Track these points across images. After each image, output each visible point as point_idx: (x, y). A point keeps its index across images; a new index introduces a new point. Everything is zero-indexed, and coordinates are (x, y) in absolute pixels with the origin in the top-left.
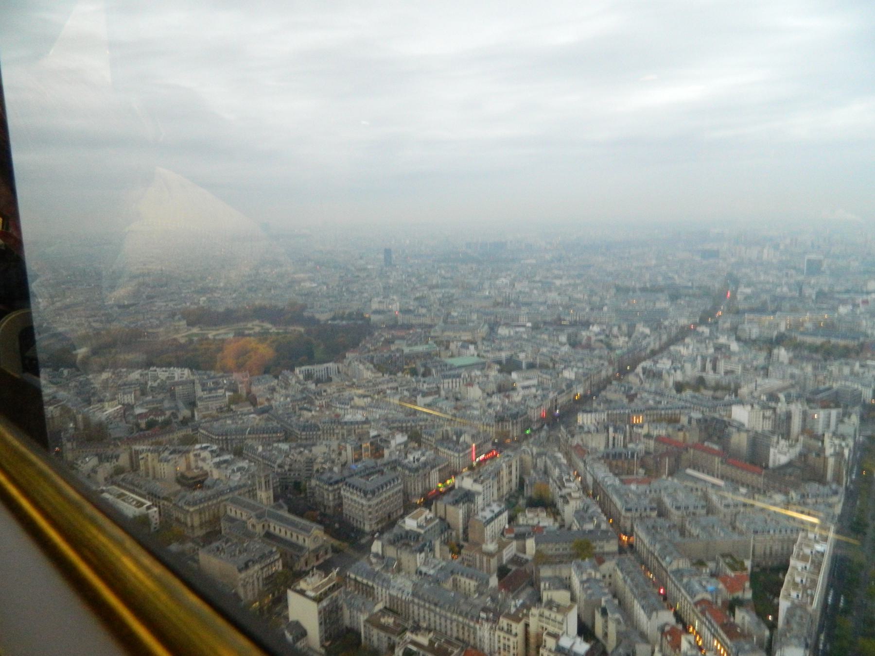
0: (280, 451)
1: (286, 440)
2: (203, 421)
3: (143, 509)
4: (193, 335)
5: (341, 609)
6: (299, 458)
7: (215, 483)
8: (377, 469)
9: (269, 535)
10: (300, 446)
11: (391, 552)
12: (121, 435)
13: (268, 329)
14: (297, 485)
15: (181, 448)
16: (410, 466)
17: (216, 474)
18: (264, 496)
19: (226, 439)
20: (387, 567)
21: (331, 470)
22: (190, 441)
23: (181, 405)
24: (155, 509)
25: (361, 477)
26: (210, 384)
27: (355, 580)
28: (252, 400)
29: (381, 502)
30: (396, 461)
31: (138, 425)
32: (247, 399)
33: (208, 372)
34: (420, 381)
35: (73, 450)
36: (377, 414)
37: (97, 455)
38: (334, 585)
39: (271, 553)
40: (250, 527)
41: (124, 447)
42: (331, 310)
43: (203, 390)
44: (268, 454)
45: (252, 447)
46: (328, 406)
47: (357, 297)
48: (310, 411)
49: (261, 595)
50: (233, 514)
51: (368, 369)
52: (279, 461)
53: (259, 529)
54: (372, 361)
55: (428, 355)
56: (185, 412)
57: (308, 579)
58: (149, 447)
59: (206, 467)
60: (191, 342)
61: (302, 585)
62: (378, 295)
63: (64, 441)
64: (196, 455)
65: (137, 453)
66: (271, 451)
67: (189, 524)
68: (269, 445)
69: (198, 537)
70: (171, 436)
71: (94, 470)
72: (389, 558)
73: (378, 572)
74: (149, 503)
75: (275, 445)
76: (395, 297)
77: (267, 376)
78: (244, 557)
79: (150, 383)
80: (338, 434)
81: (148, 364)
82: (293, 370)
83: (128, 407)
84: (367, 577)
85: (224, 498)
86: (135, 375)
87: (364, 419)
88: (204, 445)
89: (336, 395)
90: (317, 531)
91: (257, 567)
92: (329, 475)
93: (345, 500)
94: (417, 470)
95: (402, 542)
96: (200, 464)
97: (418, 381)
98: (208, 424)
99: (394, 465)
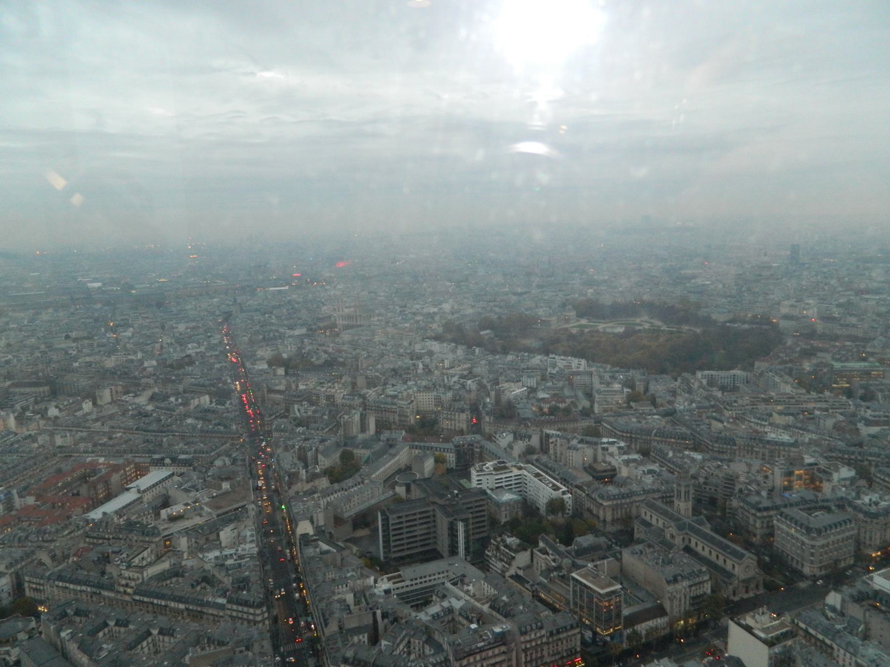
0: (693, 460)
1: (695, 449)
4: (586, 326)
5: (794, 661)
6: (717, 472)
7: (624, 483)
8: (821, 504)
9: (688, 550)
10: (716, 459)
11: (855, 611)
12: (530, 416)
14: (713, 501)
15: (589, 438)
16: (865, 508)
18: (683, 506)
19: (631, 437)
20: (851, 629)
21: (758, 493)
22: (594, 433)
23: (580, 394)
25: (801, 510)
26: (607, 376)
27: (806, 631)
29: (827, 545)
30: (842, 498)
31: (541, 409)
34: (861, 406)
35: (490, 423)
36: (807, 437)
38: (787, 632)
39: (700, 571)
40: (668, 536)
42: (730, 312)
43: (601, 383)
44: (679, 461)
45: (661, 451)
46: (738, 419)
47: (761, 299)
48: (722, 422)
49: (687, 615)
50: (648, 518)
51: (786, 383)
52: (692, 471)
53: (678, 541)
54: (790, 373)
55: (867, 373)
56: (586, 403)
57: (757, 616)
58: (558, 433)
59: (614, 463)
60: (582, 333)
61: (749, 621)
62: (788, 297)
63: (484, 415)
64: (603, 449)
65: (548, 436)
66: (682, 458)
67: (602, 518)
68: (679, 451)
70: (575, 425)
71: (510, 446)
72: (851, 617)
73: (839, 631)
74: (564, 489)
75: (687, 453)
76: (811, 301)
77: (664, 376)
78: (670, 570)
79: (549, 370)
80: (757, 452)
81: (547, 353)
82: (694, 373)
84: (826, 635)
85: (637, 499)
86: (537, 360)
87: (792, 441)
88: (611, 440)
89: (749, 407)
90: (750, 559)
91: (686, 583)
92: (757, 498)
93: (777, 532)
94: (876, 516)
95: (870, 602)
96: (608, 459)
97: (857, 406)
98: (612, 419)
99: (842, 504)
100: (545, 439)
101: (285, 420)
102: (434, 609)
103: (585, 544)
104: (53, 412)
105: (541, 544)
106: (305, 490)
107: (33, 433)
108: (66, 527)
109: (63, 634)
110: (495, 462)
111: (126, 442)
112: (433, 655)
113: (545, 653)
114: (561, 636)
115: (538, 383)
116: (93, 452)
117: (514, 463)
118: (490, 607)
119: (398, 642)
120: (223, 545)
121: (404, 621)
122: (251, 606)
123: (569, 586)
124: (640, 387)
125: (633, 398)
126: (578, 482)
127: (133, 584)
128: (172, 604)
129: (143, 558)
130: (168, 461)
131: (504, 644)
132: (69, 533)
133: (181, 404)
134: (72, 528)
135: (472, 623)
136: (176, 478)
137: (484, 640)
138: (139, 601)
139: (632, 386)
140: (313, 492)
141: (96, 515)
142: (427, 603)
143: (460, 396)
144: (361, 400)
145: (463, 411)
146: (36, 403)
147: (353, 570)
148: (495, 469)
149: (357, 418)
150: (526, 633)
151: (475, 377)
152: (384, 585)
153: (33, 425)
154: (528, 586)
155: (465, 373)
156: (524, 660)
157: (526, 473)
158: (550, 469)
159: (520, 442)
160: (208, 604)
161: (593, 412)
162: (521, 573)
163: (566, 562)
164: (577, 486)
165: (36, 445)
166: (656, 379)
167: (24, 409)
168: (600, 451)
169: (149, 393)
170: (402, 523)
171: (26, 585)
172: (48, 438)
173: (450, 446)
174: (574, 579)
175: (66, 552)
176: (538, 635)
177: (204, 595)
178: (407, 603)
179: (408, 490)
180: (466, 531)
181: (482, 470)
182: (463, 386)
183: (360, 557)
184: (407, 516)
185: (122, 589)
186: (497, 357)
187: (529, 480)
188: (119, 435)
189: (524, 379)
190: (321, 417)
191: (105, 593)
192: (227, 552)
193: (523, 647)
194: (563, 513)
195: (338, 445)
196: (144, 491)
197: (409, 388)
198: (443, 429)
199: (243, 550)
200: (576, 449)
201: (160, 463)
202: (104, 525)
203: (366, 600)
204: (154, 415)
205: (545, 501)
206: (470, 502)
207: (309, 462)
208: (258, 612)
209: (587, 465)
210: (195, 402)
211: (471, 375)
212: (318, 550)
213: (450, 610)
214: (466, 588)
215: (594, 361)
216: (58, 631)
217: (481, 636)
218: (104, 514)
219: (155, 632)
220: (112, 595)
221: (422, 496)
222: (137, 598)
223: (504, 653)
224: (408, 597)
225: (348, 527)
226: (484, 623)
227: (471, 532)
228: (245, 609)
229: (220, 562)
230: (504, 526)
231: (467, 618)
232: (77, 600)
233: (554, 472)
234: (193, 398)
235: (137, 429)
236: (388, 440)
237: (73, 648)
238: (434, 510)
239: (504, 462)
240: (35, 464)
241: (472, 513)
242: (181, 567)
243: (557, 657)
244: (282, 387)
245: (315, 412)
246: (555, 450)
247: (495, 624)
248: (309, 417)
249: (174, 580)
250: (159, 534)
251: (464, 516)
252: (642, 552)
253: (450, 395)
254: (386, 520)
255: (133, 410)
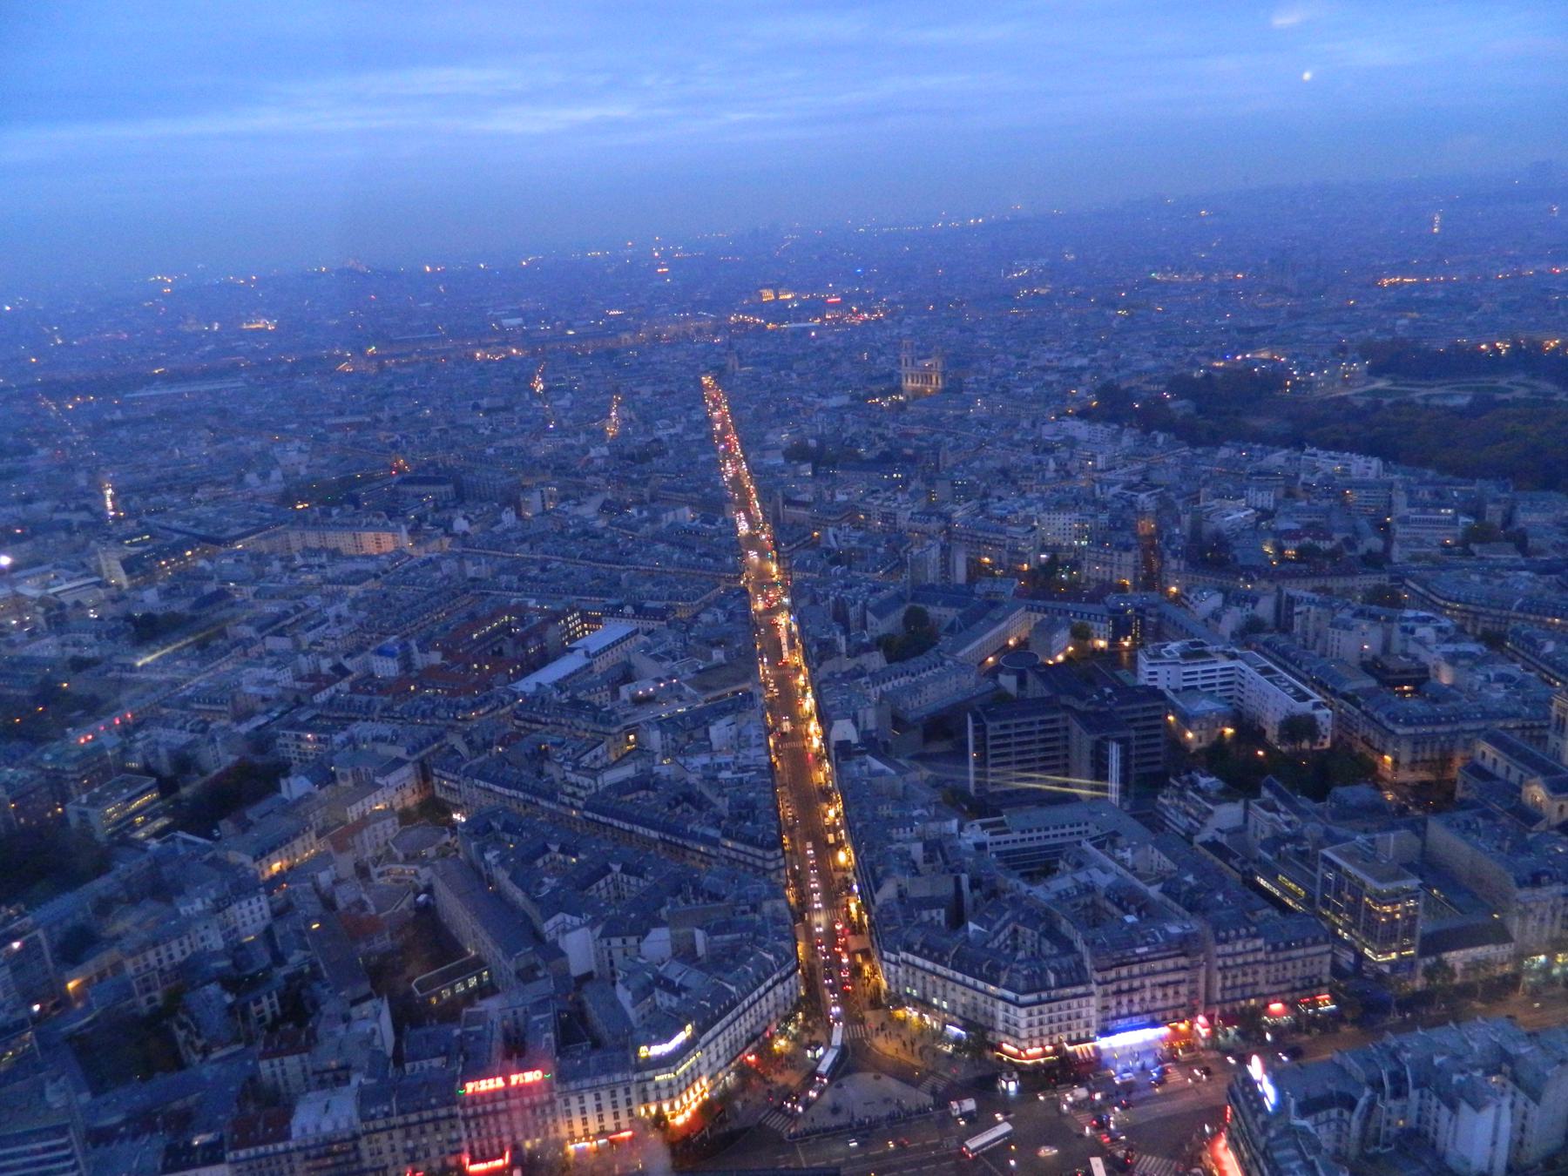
2: (1414, 565)
3: (1305, 707)
7: (1442, 695)
13: (1547, 394)
17: (1446, 677)
23: (1363, 523)
24: (1328, 711)
26: (1425, 494)
28: (1520, 541)
32: (1508, 539)
33: (1419, 470)
37: (1220, 590)
41: (1264, 583)
43: (1410, 505)
56: (1374, 543)
58: (1312, 595)
59: (1424, 656)
60: (1377, 406)
64: (1404, 630)
65: (1292, 601)
69: (1405, 784)
71: (1216, 616)
74: (1318, 698)
77: (1552, 493)
79: (1303, 476)
83: (1266, 514)
86: (1278, 458)
96: (1413, 648)
98: (1427, 575)
100: (1285, 609)
101: (813, 553)
102: (1063, 883)
103: (1353, 802)
104: (460, 525)
105: (1266, 794)
106: (845, 669)
107: (433, 556)
108: (486, 700)
109: (488, 856)
110: (1186, 642)
111: (567, 576)
112: (1056, 957)
113: (1261, 977)
114: (1294, 953)
115: (1277, 502)
116: (519, 590)
117: (1220, 648)
118: (1162, 891)
119: (997, 926)
120: (715, 747)
121: (1007, 896)
122: (761, 847)
123: (1315, 870)
124: (1494, 514)
125: (1480, 535)
126: (1347, 688)
127: (582, 794)
128: (640, 830)
129: (596, 757)
130: (629, 610)
131: (1185, 955)
132: (491, 710)
133: (646, 520)
134: (494, 703)
135: (1129, 913)
136: (642, 638)
137: (1147, 944)
138: (592, 820)
139: (1477, 514)
140: (859, 673)
141: (527, 685)
142: (1049, 871)
143: (1124, 522)
144: (942, 523)
145: (1127, 548)
146: (437, 509)
147: (923, 806)
148: (1185, 655)
149: (935, 553)
150: (1225, 941)
151: (1154, 487)
152: (974, 834)
153: (434, 545)
154: (1231, 861)
155: (1136, 479)
156: (1219, 985)
157: (1243, 666)
158: (1293, 662)
159: (1235, 609)
160: (693, 836)
161: (1390, 561)
162: (1223, 839)
163: (1313, 829)
164: (1345, 697)
165: (438, 575)
166: (1531, 499)
167: (421, 519)
168: (1397, 634)
169: (597, 500)
170: (1009, 736)
171: (435, 780)
172: (455, 565)
173: (1100, 608)
174: (1326, 859)
175: (488, 737)
176: (1250, 946)
177: (689, 821)
178: (1014, 868)
179: (1022, 682)
180: (1125, 760)
181: (1159, 656)
182: (1131, 504)
183: (934, 787)
184: (1017, 726)
185: (567, 800)
186: (1199, 451)
187: (1248, 678)
188: (555, 565)
189: (1251, 493)
190: (874, 551)
191: (545, 804)
192: (720, 759)
193: (1220, 963)
194: (1313, 741)
195: (899, 598)
196: (595, 655)
197: (1030, 505)
198: (1088, 579)
199: (746, 757)
200: (1348, 627)
201: (615, 612)
202: (538, 701)
203: (943, 855)
204: (607, 535)
205: (1279, 718)
206: (1134, 711)
207: (852, 625)
208: (770, 855)
209: (1369, 659)
210: (668, 518)
211: (1146, 483)
212: (865, 768)
213: (1089, 889)
214: (1119, 854)
215: (1397, 461)
216: (482, 850)
217: (1144, 937)
218: (539, 685)
219: (617, 868)
220: (553, 806)
221: (1047, 694)
222: (589, 815)
223: (1184, 968)
224: (1015, 859)
225: (916, 736)
226: (1149, 916)
227: (1133, 762)
228: (750, 849)
229: (710, 773)
230: (1194, 755)
231: (1119, 905)
232: (506, 810)
233: (1299, 667)
234: (666, 510)
235: (582, 557)
236: (988, 594)
237: (502, 876)
238: (1065, 719)
239: (1202, 644)
240: (439, 603)
241: (1136, 729)
242: (652, 776)
243: (1283, 987)
244: (807, 497)
245: (862, 540)
246: (1304, 627)
247: (1169, 920)
248: (853, 549)
249: (642, 794)
250: (618, 722)
251: (1122, 734)
252: (1468, 824)
253: (1104, 518)
254: (980, 729)
255: (575, 526)
